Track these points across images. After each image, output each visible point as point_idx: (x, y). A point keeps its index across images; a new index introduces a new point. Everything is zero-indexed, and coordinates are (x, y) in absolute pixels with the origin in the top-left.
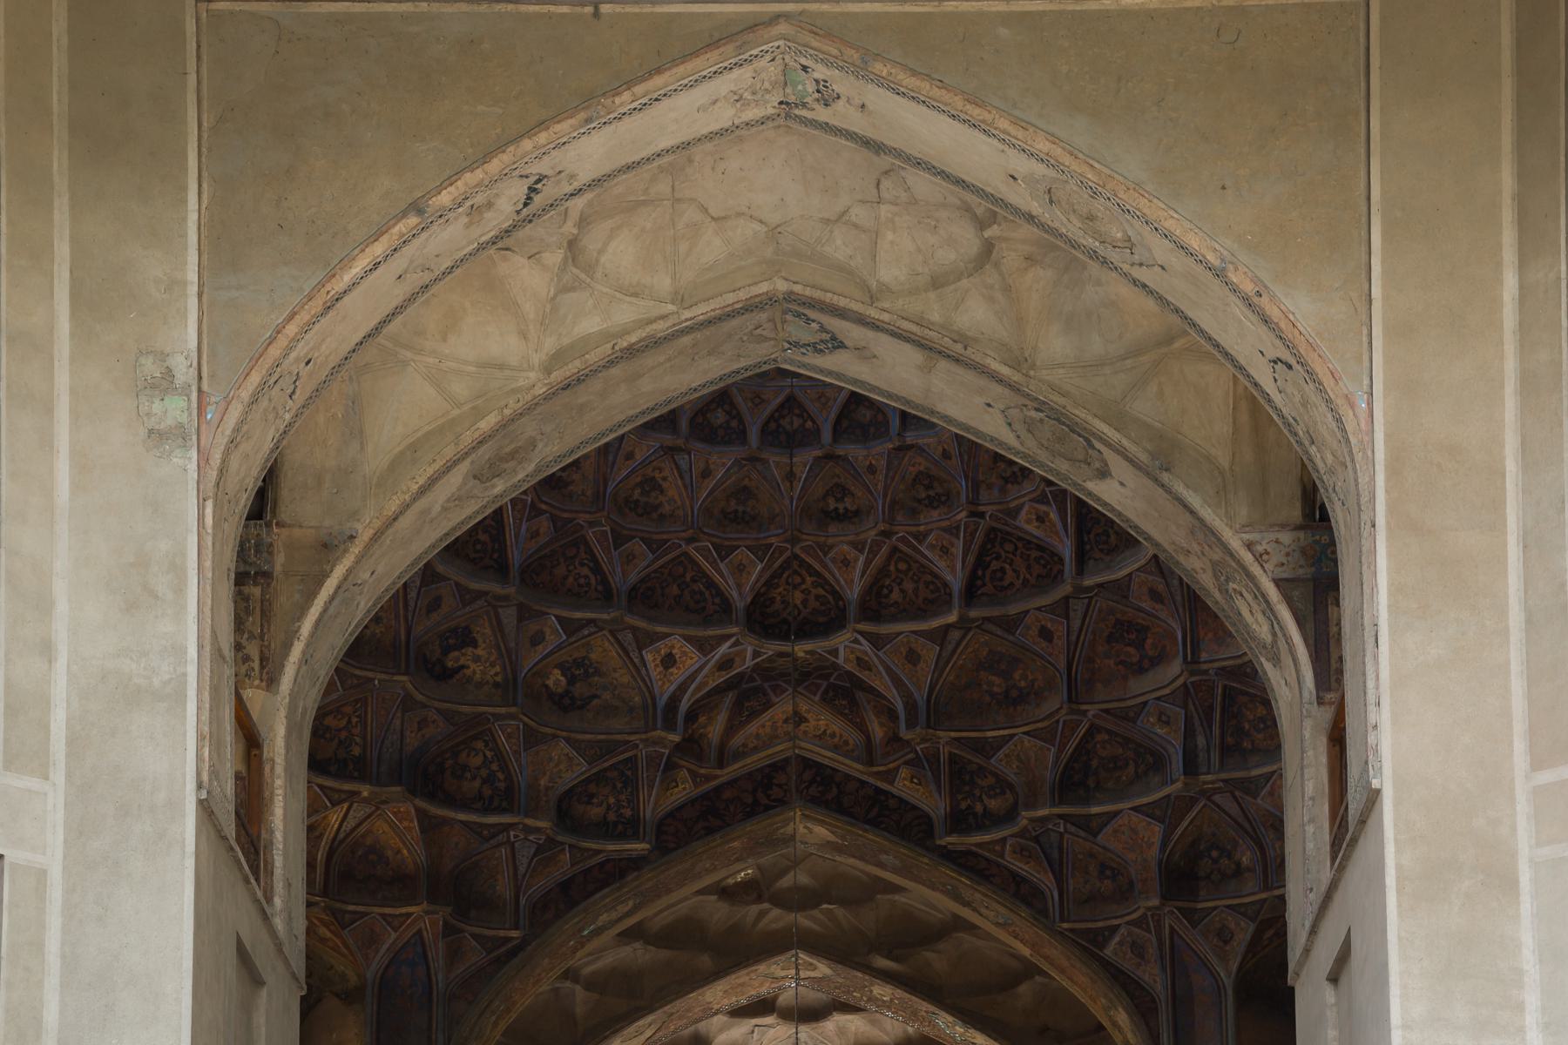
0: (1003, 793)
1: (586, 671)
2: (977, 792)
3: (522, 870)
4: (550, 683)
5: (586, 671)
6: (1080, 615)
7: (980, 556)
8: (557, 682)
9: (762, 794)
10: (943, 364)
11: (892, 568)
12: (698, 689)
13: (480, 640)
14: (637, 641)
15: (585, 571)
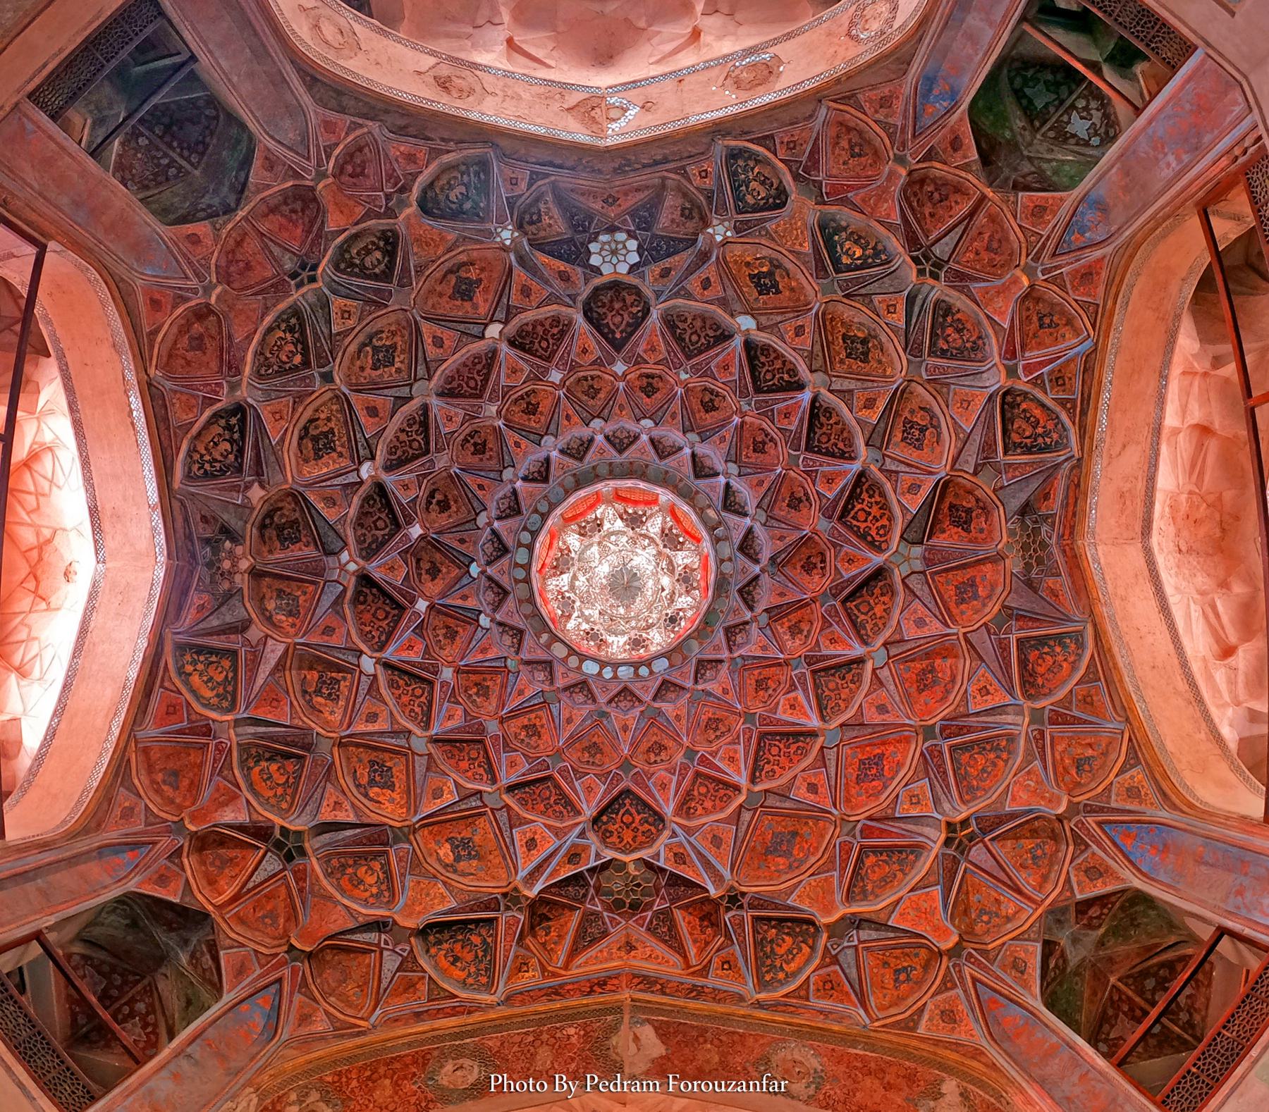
0: (800, 949)
1: (469, 853)
3: (384, 984)
4: (441, 853)
5: (469, 853)
6: (834, 763)
7: (756, 761)
8: (446, 855)
11: (696, 793)
12: (551, 875)
15: (481, 771)
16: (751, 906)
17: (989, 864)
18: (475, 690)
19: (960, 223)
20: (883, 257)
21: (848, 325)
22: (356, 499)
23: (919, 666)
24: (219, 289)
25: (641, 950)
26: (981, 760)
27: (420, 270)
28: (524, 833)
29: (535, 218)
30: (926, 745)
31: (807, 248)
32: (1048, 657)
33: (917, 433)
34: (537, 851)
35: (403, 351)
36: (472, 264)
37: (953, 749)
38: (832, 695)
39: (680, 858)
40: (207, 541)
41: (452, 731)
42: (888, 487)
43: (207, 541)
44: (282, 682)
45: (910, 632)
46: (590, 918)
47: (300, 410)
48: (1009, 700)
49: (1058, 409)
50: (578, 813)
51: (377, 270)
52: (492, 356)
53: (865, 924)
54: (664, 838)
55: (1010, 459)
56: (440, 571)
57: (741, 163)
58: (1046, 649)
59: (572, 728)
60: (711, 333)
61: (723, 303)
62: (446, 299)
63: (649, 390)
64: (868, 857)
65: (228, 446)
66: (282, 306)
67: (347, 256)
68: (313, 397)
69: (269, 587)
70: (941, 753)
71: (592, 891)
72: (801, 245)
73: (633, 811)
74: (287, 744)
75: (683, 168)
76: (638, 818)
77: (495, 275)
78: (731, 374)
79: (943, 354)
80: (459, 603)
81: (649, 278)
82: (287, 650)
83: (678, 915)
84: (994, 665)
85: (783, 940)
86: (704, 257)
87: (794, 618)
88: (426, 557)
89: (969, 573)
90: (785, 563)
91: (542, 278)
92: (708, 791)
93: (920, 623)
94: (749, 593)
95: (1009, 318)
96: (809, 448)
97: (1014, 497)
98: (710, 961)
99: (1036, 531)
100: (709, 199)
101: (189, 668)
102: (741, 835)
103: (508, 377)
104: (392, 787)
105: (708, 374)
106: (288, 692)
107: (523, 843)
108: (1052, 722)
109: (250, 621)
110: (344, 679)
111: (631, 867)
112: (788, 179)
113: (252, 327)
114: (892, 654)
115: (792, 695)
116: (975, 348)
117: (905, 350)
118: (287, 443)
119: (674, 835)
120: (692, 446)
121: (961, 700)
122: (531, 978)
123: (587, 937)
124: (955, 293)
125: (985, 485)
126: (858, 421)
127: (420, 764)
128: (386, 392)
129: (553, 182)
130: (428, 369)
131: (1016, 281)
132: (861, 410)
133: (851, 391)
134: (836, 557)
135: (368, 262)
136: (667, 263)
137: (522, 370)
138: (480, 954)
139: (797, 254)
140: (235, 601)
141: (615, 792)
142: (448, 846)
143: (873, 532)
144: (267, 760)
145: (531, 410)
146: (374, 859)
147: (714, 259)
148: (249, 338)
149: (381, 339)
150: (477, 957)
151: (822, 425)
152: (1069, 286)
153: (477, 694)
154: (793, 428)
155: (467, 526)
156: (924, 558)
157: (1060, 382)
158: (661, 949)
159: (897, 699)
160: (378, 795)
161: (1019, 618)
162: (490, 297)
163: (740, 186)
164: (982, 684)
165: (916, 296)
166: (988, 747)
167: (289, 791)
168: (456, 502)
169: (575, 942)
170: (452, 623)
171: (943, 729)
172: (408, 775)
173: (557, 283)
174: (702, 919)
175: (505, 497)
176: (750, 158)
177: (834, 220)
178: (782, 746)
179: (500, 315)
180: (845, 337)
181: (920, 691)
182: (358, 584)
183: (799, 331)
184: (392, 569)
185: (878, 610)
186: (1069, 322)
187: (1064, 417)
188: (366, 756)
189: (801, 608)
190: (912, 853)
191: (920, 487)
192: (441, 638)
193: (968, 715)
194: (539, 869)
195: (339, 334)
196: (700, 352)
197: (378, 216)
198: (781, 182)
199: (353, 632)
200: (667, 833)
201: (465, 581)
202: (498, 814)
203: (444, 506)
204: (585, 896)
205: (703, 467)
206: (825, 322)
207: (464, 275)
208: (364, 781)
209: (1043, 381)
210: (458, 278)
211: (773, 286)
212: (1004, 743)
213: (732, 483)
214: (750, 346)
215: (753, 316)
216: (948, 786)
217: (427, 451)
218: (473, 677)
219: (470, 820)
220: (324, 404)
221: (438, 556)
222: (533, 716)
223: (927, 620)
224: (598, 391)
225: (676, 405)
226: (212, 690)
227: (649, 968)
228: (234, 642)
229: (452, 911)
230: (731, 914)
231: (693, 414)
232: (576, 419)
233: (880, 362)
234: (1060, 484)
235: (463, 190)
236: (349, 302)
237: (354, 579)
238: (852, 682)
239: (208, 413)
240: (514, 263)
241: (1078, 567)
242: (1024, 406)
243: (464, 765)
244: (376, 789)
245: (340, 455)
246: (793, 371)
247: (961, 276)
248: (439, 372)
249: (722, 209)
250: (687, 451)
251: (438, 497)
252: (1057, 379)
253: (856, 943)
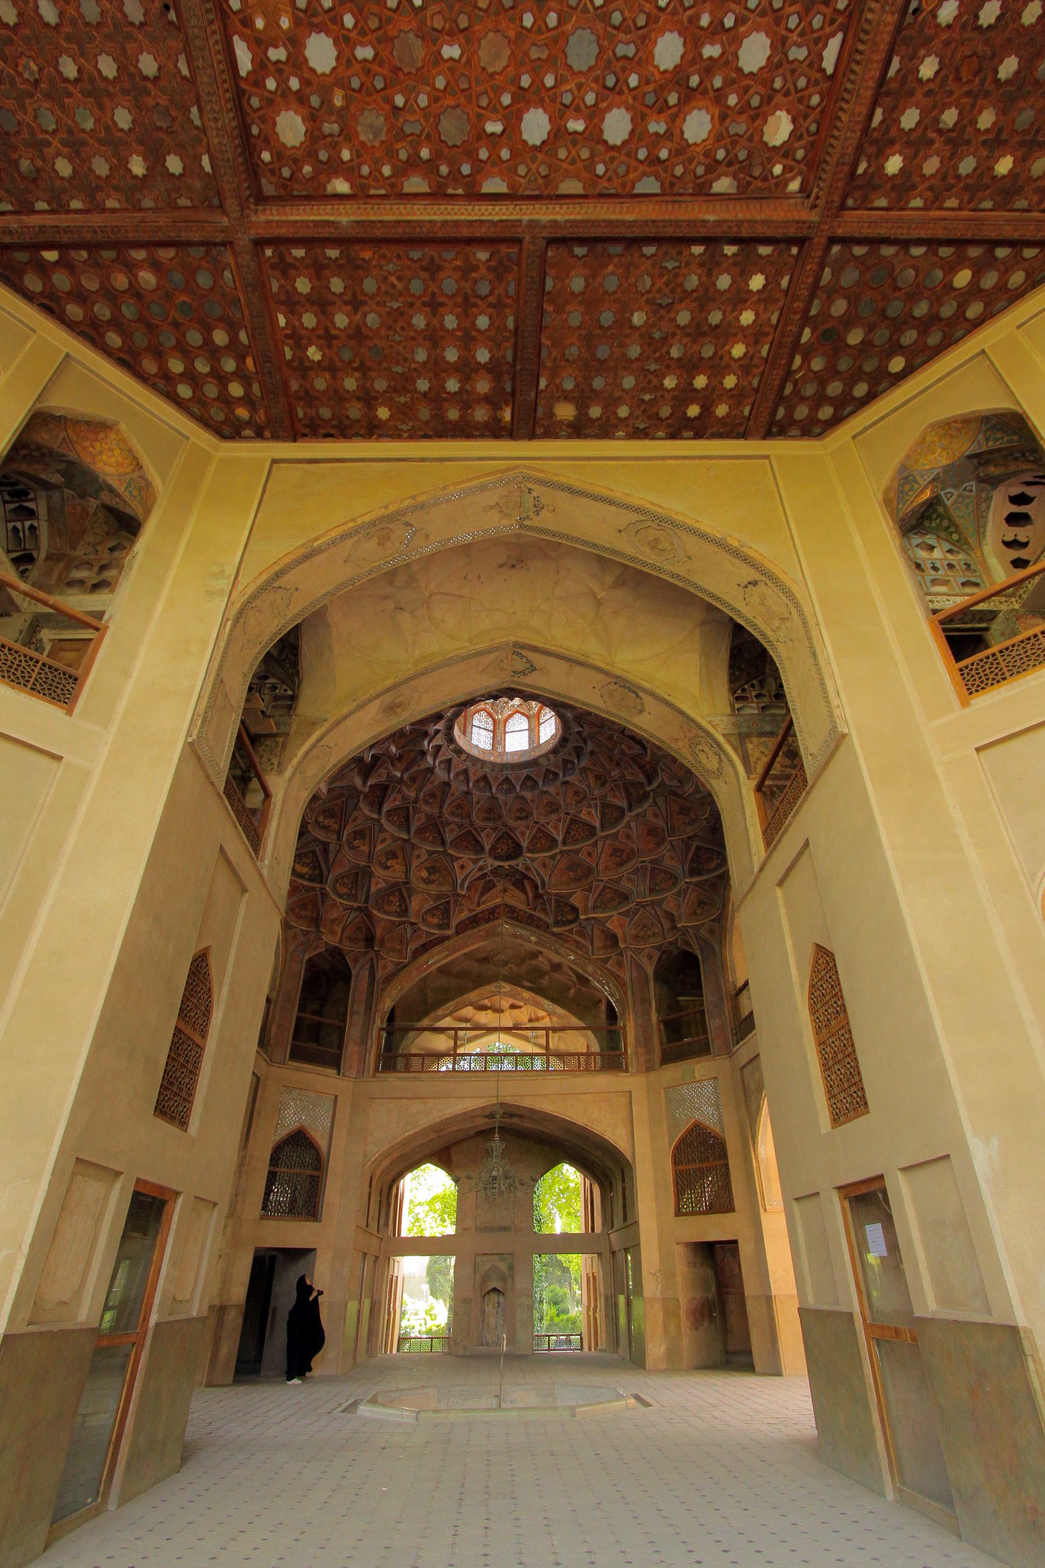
9: (492, 914)
10: (577, 669)
26: (663, 875)
50: (482, 849)
54: (520, 860)
93: (656, 816)
104: (397, 858)
122: (464, 915)
127: (408, 847)
158: (518, 893)
194: (466, 877)
227: (511, 902)
243: (427, 834)
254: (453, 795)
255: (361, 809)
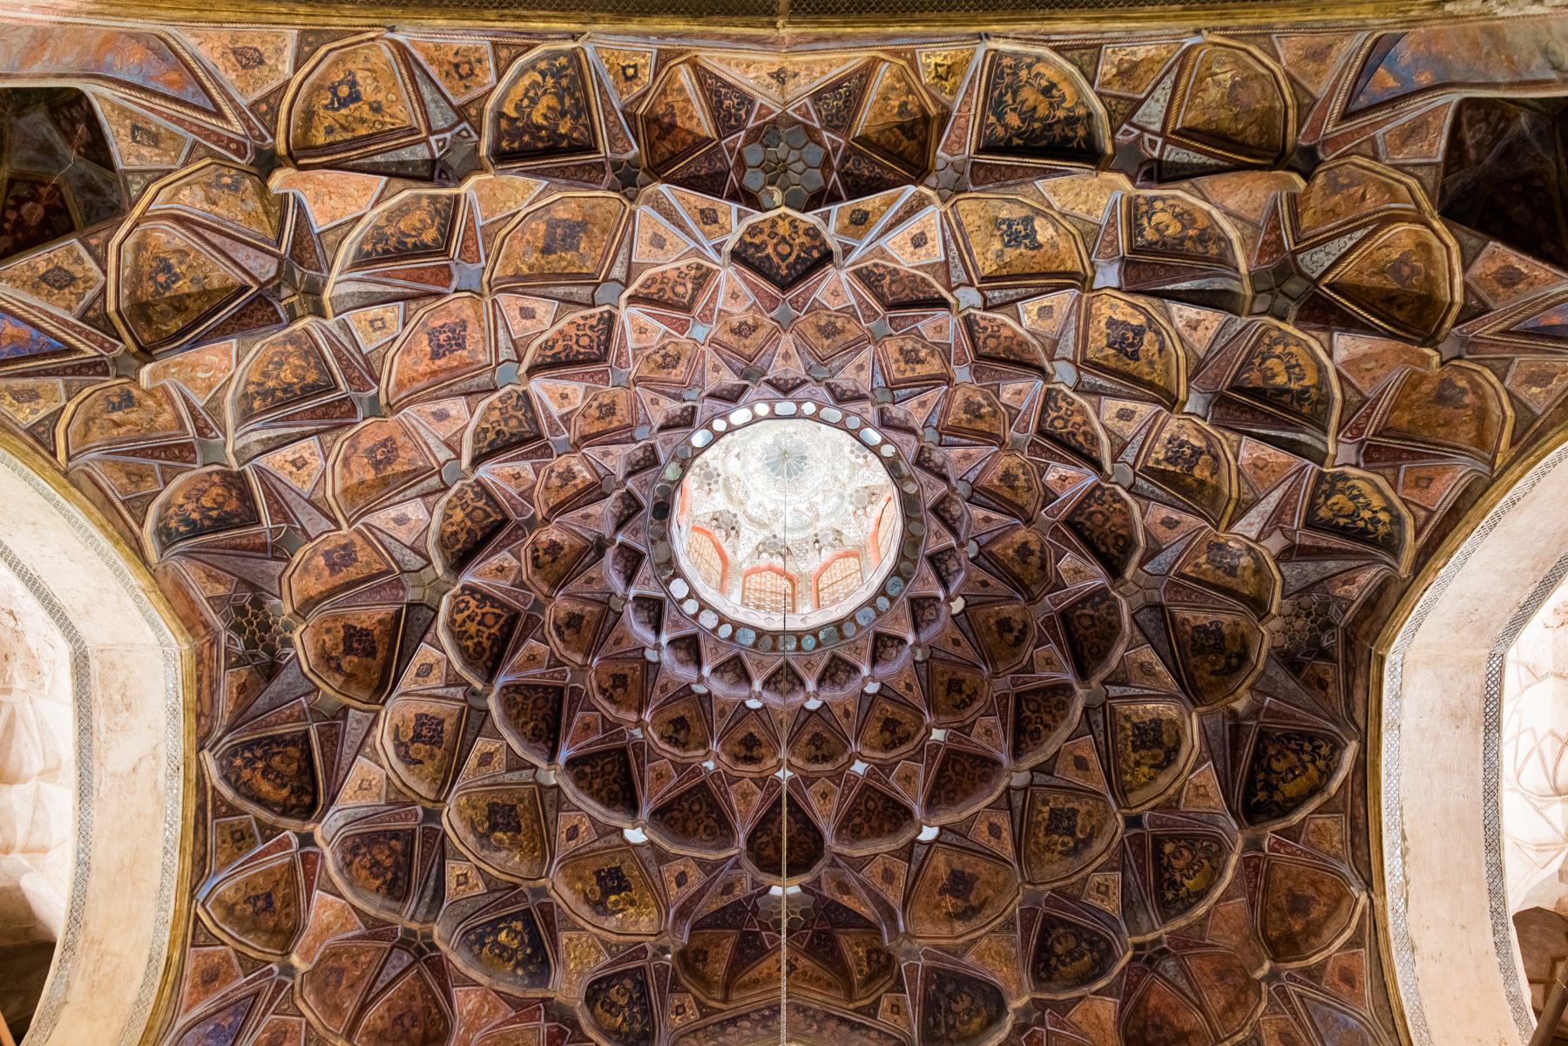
0: (518, 107)
1: (1010, 227)
2: (550, 81)
4: (1051, 231)
5: (1010, 227)
6: (501, 344)
11: (690, 286)
12: (894, 200)
13: (1102, 324)
14: (948, 272)
16: (600, 167)
17: (241, 254)
18: (983, 411)
19: (378, 995)
20: (473, 937)
21: (515, 844)
22: (1114, 663)
23: (398, 467)
24: (1259, 974)
25: (764, 74)
26: (287, 375)
27: (1009, 925)
28: (928, 255)
29: (874, 957)
30: (373, 392)
31: (563, 938)
32: (209, 505)
33: (424, 732)
34: (911, 234)
35: (1038, 824)
36: (948, 913)
37: (332, 387)
38: (511, 412)
39: (709, 217)
40: (1325, 654)
41: (1018, 377)
42: (457, 665)
43: (1325, 654)
44: (1245, 488)
45: (414, 510)
46: (840, 121)
47: (1171, 791)
48: (262, 461)
49: (239, 802)
51: (1061, 931)
52: (931, 805)
53: (422, 171)
55: (298, 727)
56: (1017, 551)
57: (637, 1026)
58: (214, 514)
59: (858, 360)
60: (677, 814)
61: (663, 858)
62: (982, 878)
63: (750, 742)
64: (434, 240)
65: (1276, 765)
66: (1181, 922)
67: (1096, 955)
68: (1152, 803)
69: (1245, 583)
70: (350, 381)
71: (835, 163)
72: (571, 940)
73: (776, 260)
74: (1253, 409)
75: (703, 1016)
76: (770, 250)
77: (923, 898)
78: (654, 769)
79: (395, 835)
80: (994, 516)
81: (747, 883)
82: (1230, 524)
83: (707, 129)
84: (289, 496)
85: (545, 116)
86: (682, 913)
87: (569, 491)
88: (1033, 569)
89: (339, 579)
90: (583, 551)
91: (870, 891)
92: (673, 289)
93: (401, 521)
94: (628, 507)
95: (314, 903)
96: (559, 691)
97: (289, 684)
98: (656, 75)
99: (250, 644)
100: (675, 981)
101: (1383, 516)
102: (624, 250)
103: (915, 773)
104: (1111, 323)
105: (681, 767)
106: (1239, 472)
107: (930, 243)
108: (189, 447)
109: (1277, 560)
110: (1157, 462)
111: (778, 197)
112: (584, 1020)
113: (1222, 908)
114: (437, 478)
115: (564, 411)
116: (354, 850)
117: (445, 834)
118: (1193, 757)
119: (717, 249)
120: (701, 680)
121: (330, 449)
123: (843, 97)
124: (385, 915)
125: (330, 691)
126: (500, 737)
127: (1067, 347)
128: (1063, 783)
129: (850, 999)
130: (1009, 801)
131: (306, 956)
132: (497, 750)
133: (509, 770)
134: (520, 571)
135: (1072, 943)
136: (727, 900)
137: (898, 779)
138: (1008, 98)
139: (575, 928)
140: (1296, 585)
141: (800, 288)
142: (1040, 238)
143: (473, 603)
144: (1289, 391)
145: (890, 725)
146: (1151, 244)
147: (672, 912)
148: (1226, 896)
149: (1064, 844)
150: (1015, 94)
151: (544, 719)
152: (235, 961)
153: (980, 406)
154: (579, 714)
155: (977, 600)
156: (404, 589)
157: (237, 836)
158: (732, 75)
159: (422, 430)
160: (1132, 315)
161: (263, 547)
162: (930, 872)
163: (639, 998)
164: (304, 471)
165: (432, 900)
166: (280, 394)
167: (1264, 348)
168: (989, 628)
169: (863, 89)
170: (1007, 494)
171: (353, 411)
172: (1086, 338)
173: (854, 883)
174: (673, 126)
175: (929, 622)
176: (627, 1035)
177: (531, 975)
178: (575, 347)
179: (919, 851)
180: (518, 829)
181: (390, 439)
182: (1125, 564)
183: (573, 833)
184: (1077, 571)
185: (459, 515)
186: (229, 910)
187: (228, 793)
188: (1142, 368)
189: (562, 504)
190: (368, 254)
191: (418, 675)
192: (1022, 477)
193: (317, 433)
194: (911, 211)
195: (1114, 869)
196: (689, 791)
197: (1054, 1005)
198: (592, 1011)
199: (1137, 514)
200: (727, 248)
201: (985, 539)
202: (964, 278)
203: (1004, 625)
204: (845, 159)
205: (687, 649)
206: (541, 847)
207: (959, 902)
208: (1149, 336)
209: (262, 834)
210: (967, 900)
211: (604, 878)
212: (256, 404)
213: (650, 636)
214: (632, 807)
215: (627, 843)
216: (331, 344)
217: (1018, 696)
218: (983, 426)
219: (1004, 272)
220: (1142, 786)
221: (1017, 569)
222: (909, 374)
223: (392, 524)
224: (812, 741)
225: (719, 726)
226: (1353, 487)
228: (1305, 538)
229: (1045, 173)
230: (631, 154)
231: (698, 715)
232: (838, 712)
233: (474, 807)
234: (225, 705)
235: (953, 1006)
236: (1098, 903)
237: (1128, 574)
238: (485, 431)
239: (1296, 818)
240: (900, 914)
241: (183, 619)
242: (285, 792)
244: (1134, 322)
245: (1127, 718)
246: (579, 779)
247: (374, 937)
248: (997, 794)
249: (662, 972)
250: (706, 671)
251: (1010, 637)
252: (243, 838)
253: (432, 139)
254: (923, 404)
255: (1146, 531)
